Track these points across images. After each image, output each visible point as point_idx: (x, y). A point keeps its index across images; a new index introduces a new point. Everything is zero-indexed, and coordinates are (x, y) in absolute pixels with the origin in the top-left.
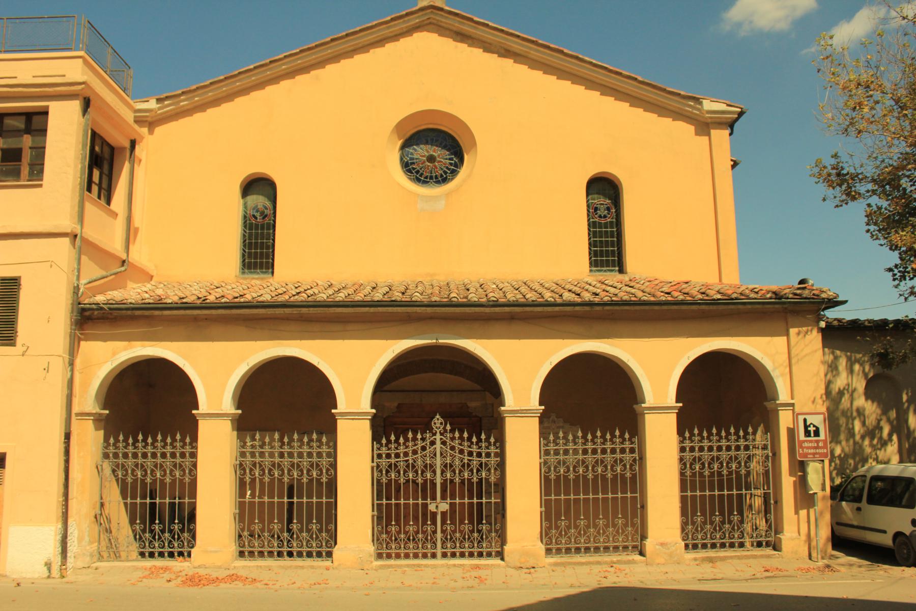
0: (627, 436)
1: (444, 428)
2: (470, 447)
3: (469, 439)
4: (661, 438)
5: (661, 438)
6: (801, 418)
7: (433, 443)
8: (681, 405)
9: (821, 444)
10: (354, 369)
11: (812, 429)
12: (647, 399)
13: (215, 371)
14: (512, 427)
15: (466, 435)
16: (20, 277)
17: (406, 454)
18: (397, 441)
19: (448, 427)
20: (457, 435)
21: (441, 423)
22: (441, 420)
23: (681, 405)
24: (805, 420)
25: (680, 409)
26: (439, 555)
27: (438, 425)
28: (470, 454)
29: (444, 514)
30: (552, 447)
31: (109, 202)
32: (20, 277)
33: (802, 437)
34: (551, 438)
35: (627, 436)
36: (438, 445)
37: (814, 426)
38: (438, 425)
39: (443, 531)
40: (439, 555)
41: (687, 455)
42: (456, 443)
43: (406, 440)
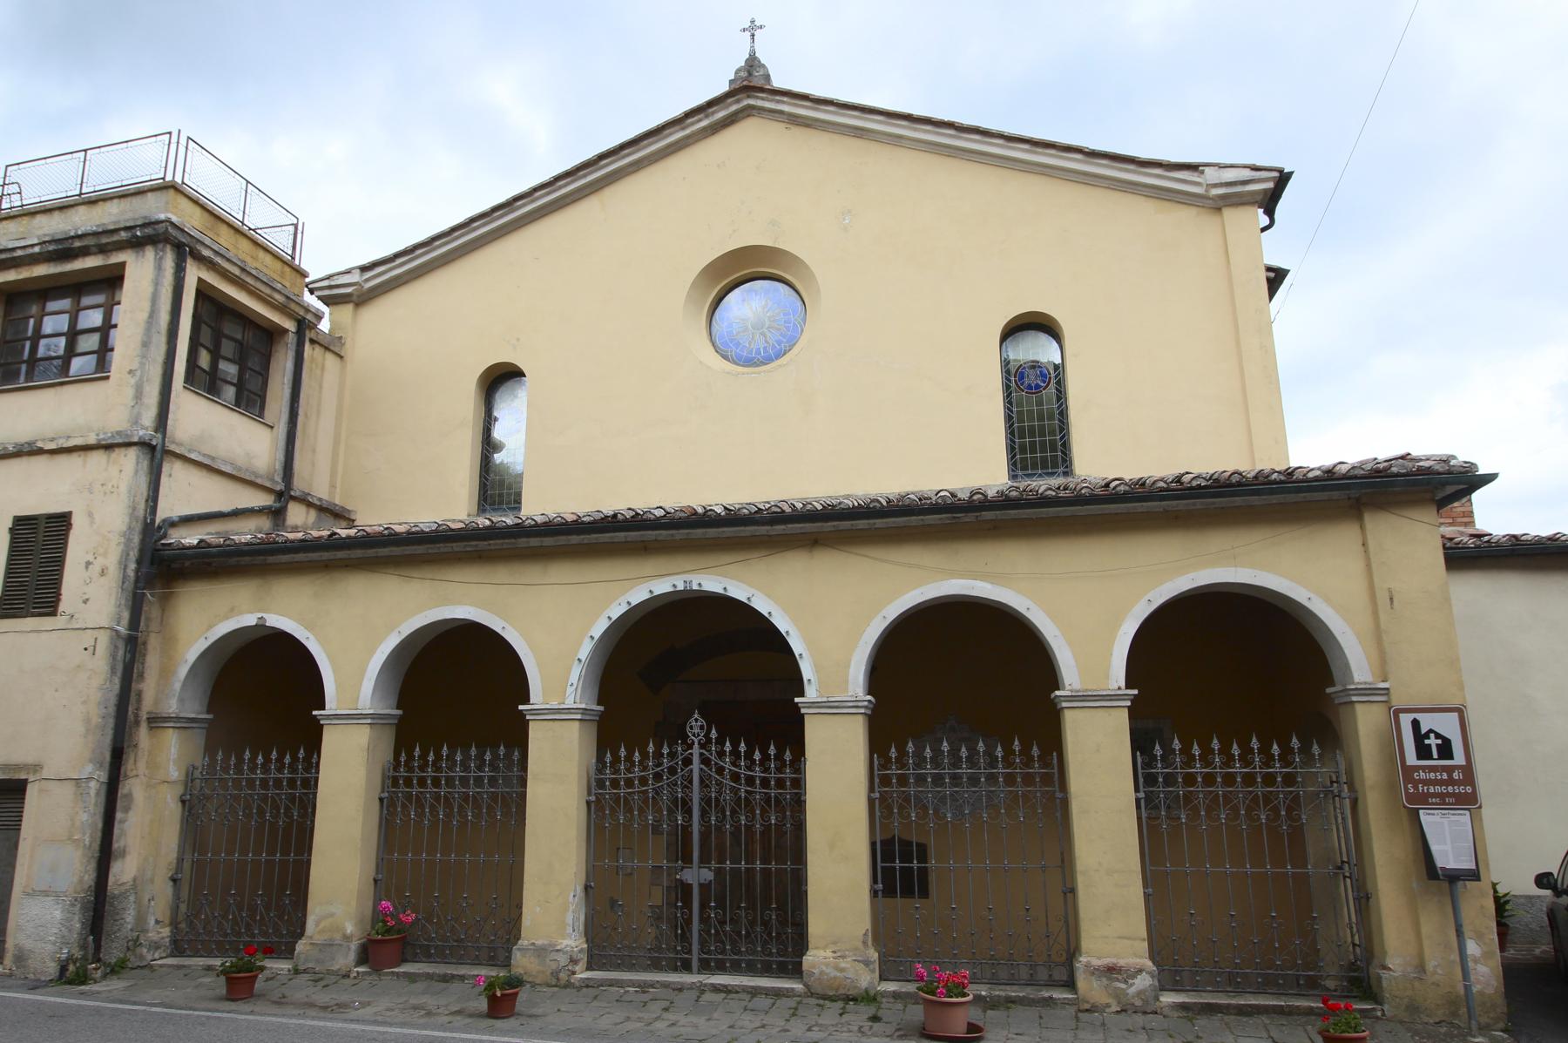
0: (1035, 751)
1: (707, 735)
2: (749, 768)
3: (749, 755)
4: (1099, 756)
5: (1099, 756)
6: (1406, 720)
7: (688, 761)
8: (1136, 692)
9: (1456, 775)
10: (557, 632)
11: (1433, 741)
12: (1067, 682)
13: (354, 641)
14: (816, 733)
15: (743, 747)
16: (70, 513)
17: (643, 781)
18: (629, 758)
19: (714, 734)
20: (728, 747)
21: (702, 727)
22: (702, 722)
23: (1136, 692)
24: (1416, 724)
25: (1135, 700)
26: (695, 964)
27: (696, 731)
28: (750, 781)
29: (704, 888)
30: (894, 771)
31: (261, 415)
32: (70, 513)
33: (1411, 758)
34: (893, 753)
35: (1035, 751)
36: (696, 765)
37: (1438, 736)
38: (696, 731)
39: (704, 920)
40: (695, 964)
41: (609, 790)
42: (727, 763)
43: (645, 755)
